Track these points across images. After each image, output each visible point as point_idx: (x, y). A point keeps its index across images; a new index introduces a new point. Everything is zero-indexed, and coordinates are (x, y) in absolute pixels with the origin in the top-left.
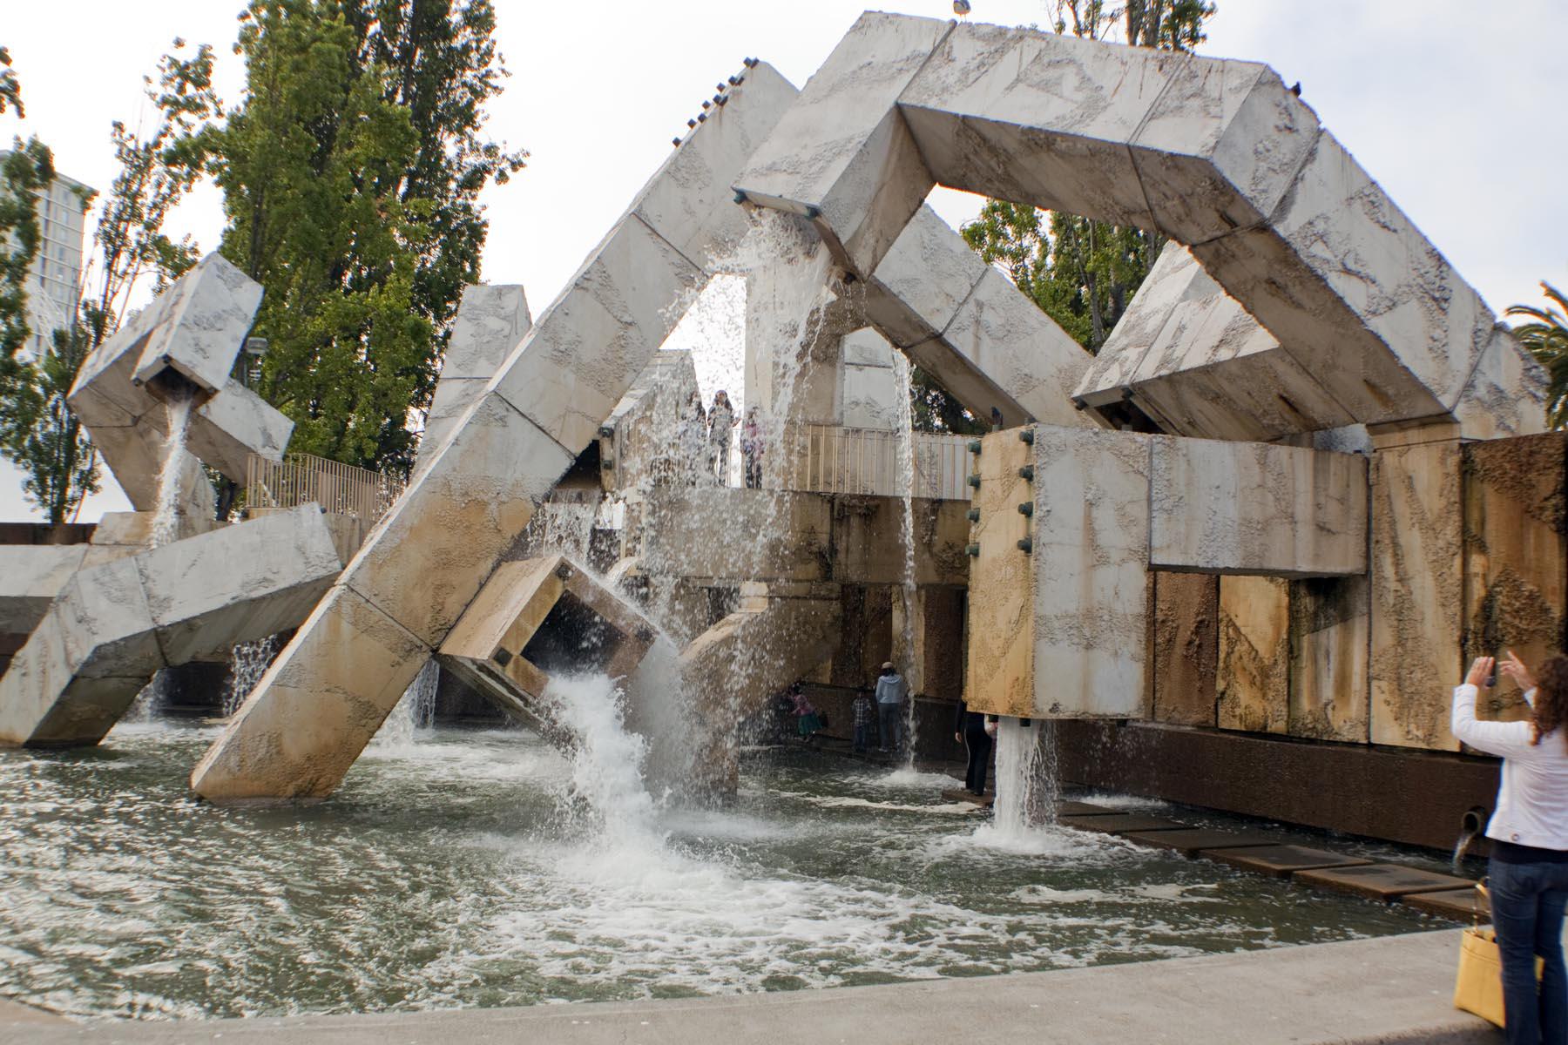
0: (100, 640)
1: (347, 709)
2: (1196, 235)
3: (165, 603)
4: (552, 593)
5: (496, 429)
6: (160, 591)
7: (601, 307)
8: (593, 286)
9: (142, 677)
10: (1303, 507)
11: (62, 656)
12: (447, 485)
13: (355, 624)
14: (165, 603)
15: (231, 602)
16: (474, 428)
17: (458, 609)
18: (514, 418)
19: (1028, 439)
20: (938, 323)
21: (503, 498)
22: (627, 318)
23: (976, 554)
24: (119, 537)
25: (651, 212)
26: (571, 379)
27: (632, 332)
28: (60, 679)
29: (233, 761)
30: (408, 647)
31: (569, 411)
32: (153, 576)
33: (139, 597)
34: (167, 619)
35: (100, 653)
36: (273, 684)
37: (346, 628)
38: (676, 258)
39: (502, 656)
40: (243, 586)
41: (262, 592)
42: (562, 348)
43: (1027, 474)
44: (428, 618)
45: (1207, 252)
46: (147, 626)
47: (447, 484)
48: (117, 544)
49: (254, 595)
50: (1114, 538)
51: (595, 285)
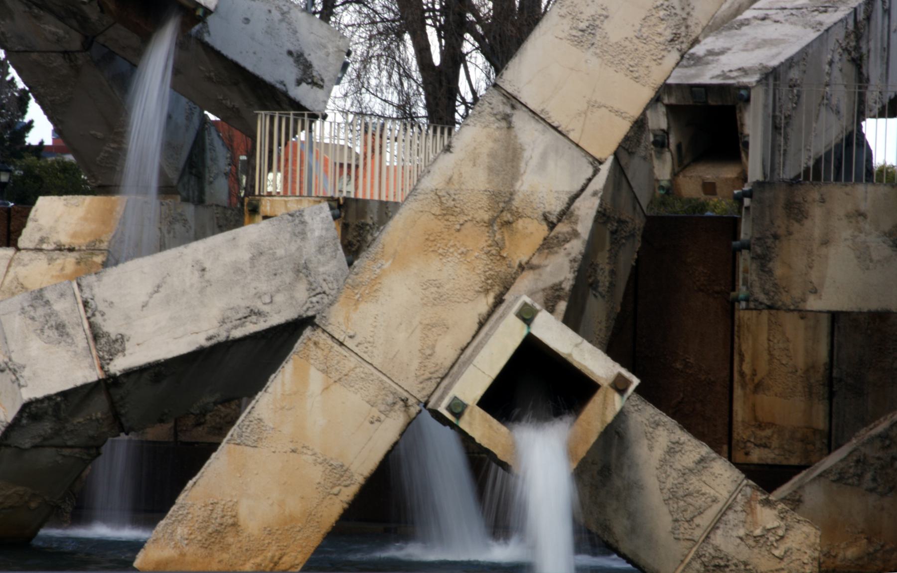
0: (27, 395)
1: (317, 474)
3: (117, 345)
6: (111, 326)
9: (87, 448)
14: (117, 345)
15: (207, 344)
17: (451, 355)
24: (65, 240)
30: (390, 399)
31: (593, 105)
32: (101, 307)
33: (81, 336)
34: (118, 366)
40: (223, 322)
41: (251, 328)
42: (583, 25)
44: (415, 364)
46: (92, 375)
48: (60, 248)
49: (238, 333)
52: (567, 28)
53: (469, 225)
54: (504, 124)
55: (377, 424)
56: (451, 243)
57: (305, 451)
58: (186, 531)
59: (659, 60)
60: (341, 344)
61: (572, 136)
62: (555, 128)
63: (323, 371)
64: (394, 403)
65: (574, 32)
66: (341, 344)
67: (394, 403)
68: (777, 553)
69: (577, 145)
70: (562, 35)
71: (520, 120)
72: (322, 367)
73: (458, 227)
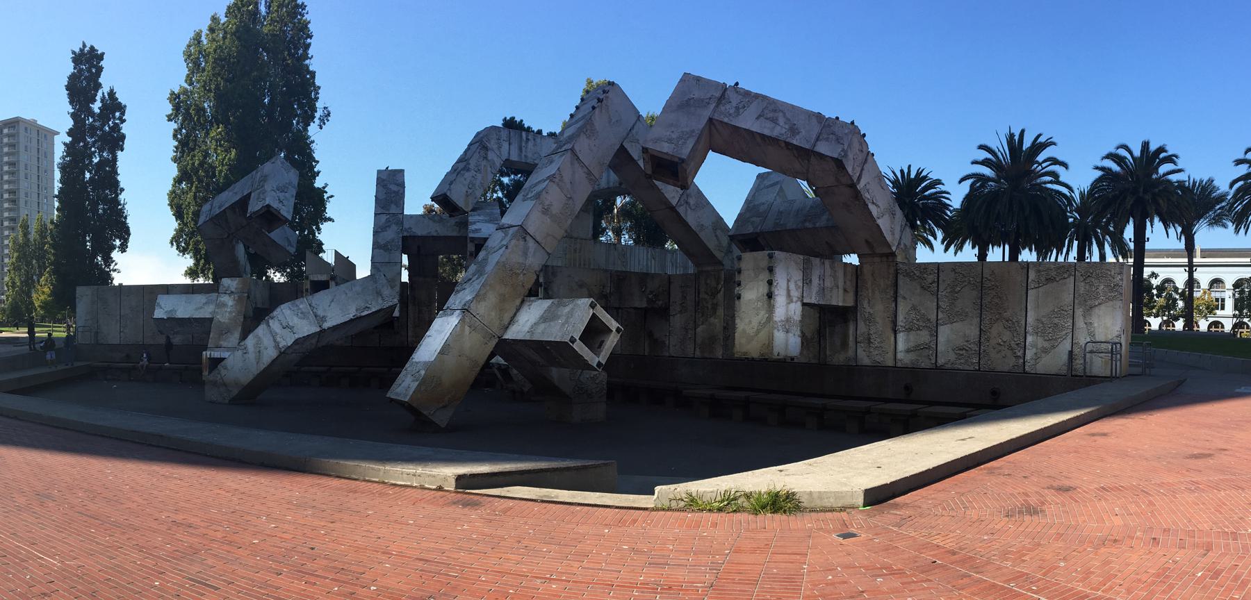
3: (323, 319)
6: (321, 313)
10: (841, 284)
11: (273, 344)
12: (504, 266)
16: (513, 242)
18: (528, 238)
19: (771, 256)
20: (674, 202)
23: (739, 298)
25: (577, 148)
28: (270, 354)
33: (311, 316)
34: (326, 325)
35: (297, 342)
37: (467, 328)
39: (573, 340)
41: (366, 313)
46: (318, 329)
47: (504, 266)
71: (528, 238)
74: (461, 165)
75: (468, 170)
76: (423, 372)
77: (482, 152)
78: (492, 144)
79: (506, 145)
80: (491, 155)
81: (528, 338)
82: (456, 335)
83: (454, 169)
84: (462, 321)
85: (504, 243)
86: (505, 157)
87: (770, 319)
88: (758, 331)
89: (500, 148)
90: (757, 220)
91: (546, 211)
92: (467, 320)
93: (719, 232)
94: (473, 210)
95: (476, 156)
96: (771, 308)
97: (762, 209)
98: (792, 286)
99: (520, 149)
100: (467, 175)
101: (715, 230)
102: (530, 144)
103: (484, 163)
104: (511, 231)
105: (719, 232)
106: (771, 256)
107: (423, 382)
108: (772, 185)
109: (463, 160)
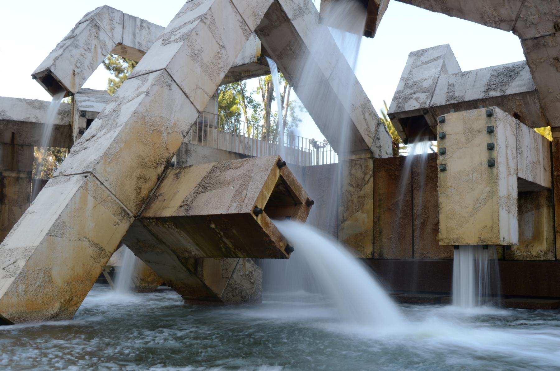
1: (90, 251)
2: (531, 33)
4: (275, 176)
5: (166, 91)
7: (211, 34)
8: (208, 22)
12: (143, 118)
13: (95, 198)
16: (156, 88)
18: (174, 86)
19: (490, 115)
21: (170, 131)
22: (221, 44)
23: (444, 170)
26: (199, 69)
27: (223, 51)
29: (21, 288)
36: (47, 234)
37: (91, 201)
38: (240, 18)
39: (257, 211)
42: (196, 52)
43: (491, 131)
44: (133, 196)
45: (530, 43)
47: (143, 118)
50: (512, 164)
51: (208, 22)
52: (190, 51)
53: (155, 131)
54: (168, 87)
55: (117, 225)
56: (149, 139)
57: (85, 239)
58: (24, 286)
59: (218, 74)
60: (102, 184)
61: (191, 99)
62: (185, 94)
63: (94, 197)
64: (124, 216)
65: (193, 54)
66: (102, 184)
67: (124, 216)
68: (252, 281)
69: (192, 103)
70: (189, 54)
72: (94, 195)
73: (151, 132)
74: (68, 42)
75: (76, 47)
76: (22, 263)
77: (94, 30)
78: (105, 24)
79: (118, 28)
80: (102, 36)
81: (182, 213)
82: (76, 209)
83: (60, 46)
84: (84, 188)
85: (144, 88)
86: (118, 40)
87: (492, 194)
88: (475, 210)
89: (112, 29)
90: (423, 97)
91: (195, 56)
92: (91, 187)
93: (367, 115)
94: (78, 93)
95: (86, 34)
96: (493, 181)
97: (426, 84)
98: (509, 152)
99: (134, 35)
100: (76, 53)
101: (363, 113)
102: (144, 32)
103: (95, 42)
104: (152, 76)
105: (367, 115)
106: (490, 115)
107: (23, 277)
108: (430, 61)
109: (72, 37)
